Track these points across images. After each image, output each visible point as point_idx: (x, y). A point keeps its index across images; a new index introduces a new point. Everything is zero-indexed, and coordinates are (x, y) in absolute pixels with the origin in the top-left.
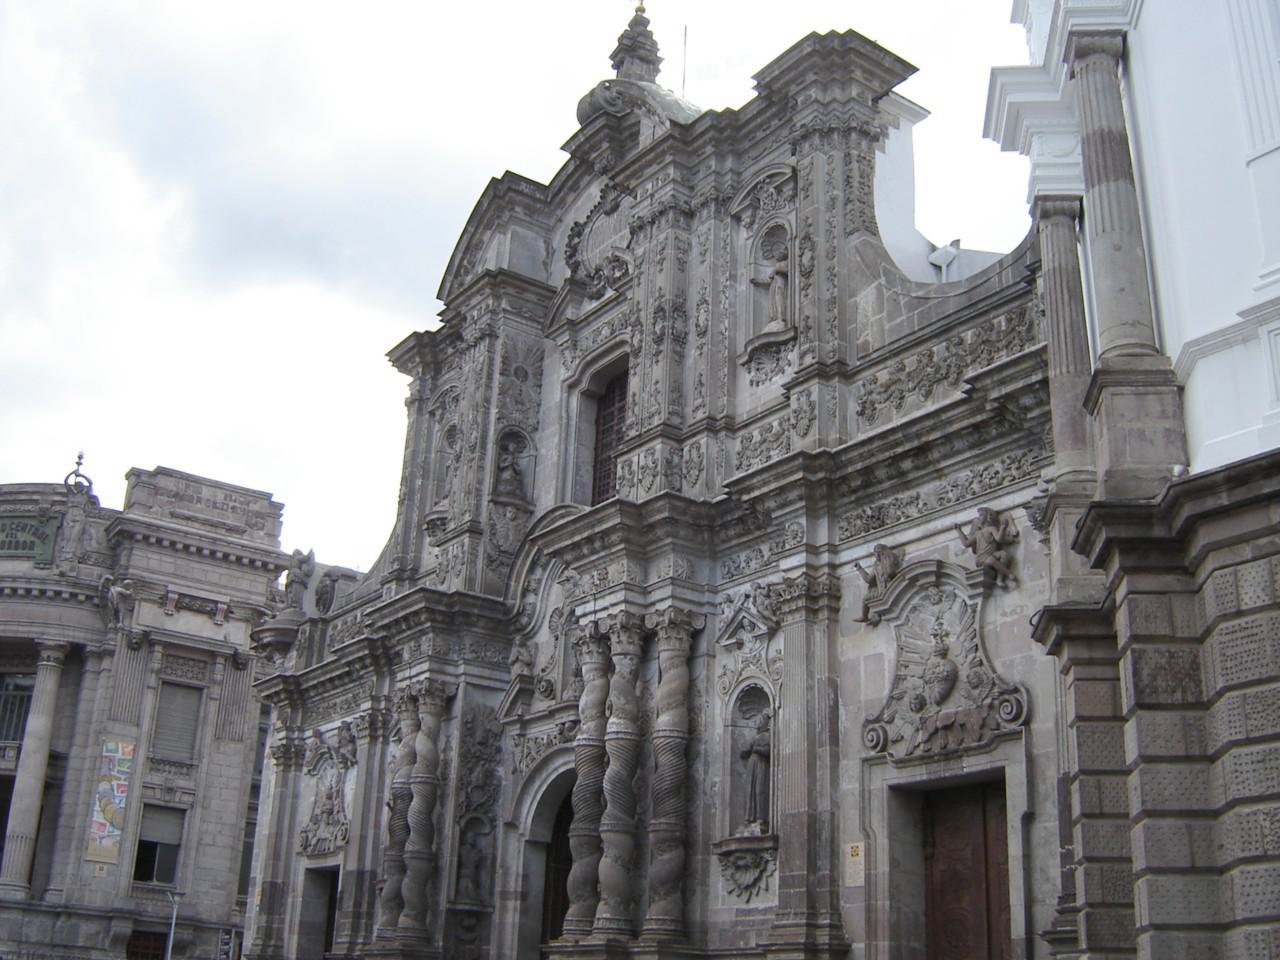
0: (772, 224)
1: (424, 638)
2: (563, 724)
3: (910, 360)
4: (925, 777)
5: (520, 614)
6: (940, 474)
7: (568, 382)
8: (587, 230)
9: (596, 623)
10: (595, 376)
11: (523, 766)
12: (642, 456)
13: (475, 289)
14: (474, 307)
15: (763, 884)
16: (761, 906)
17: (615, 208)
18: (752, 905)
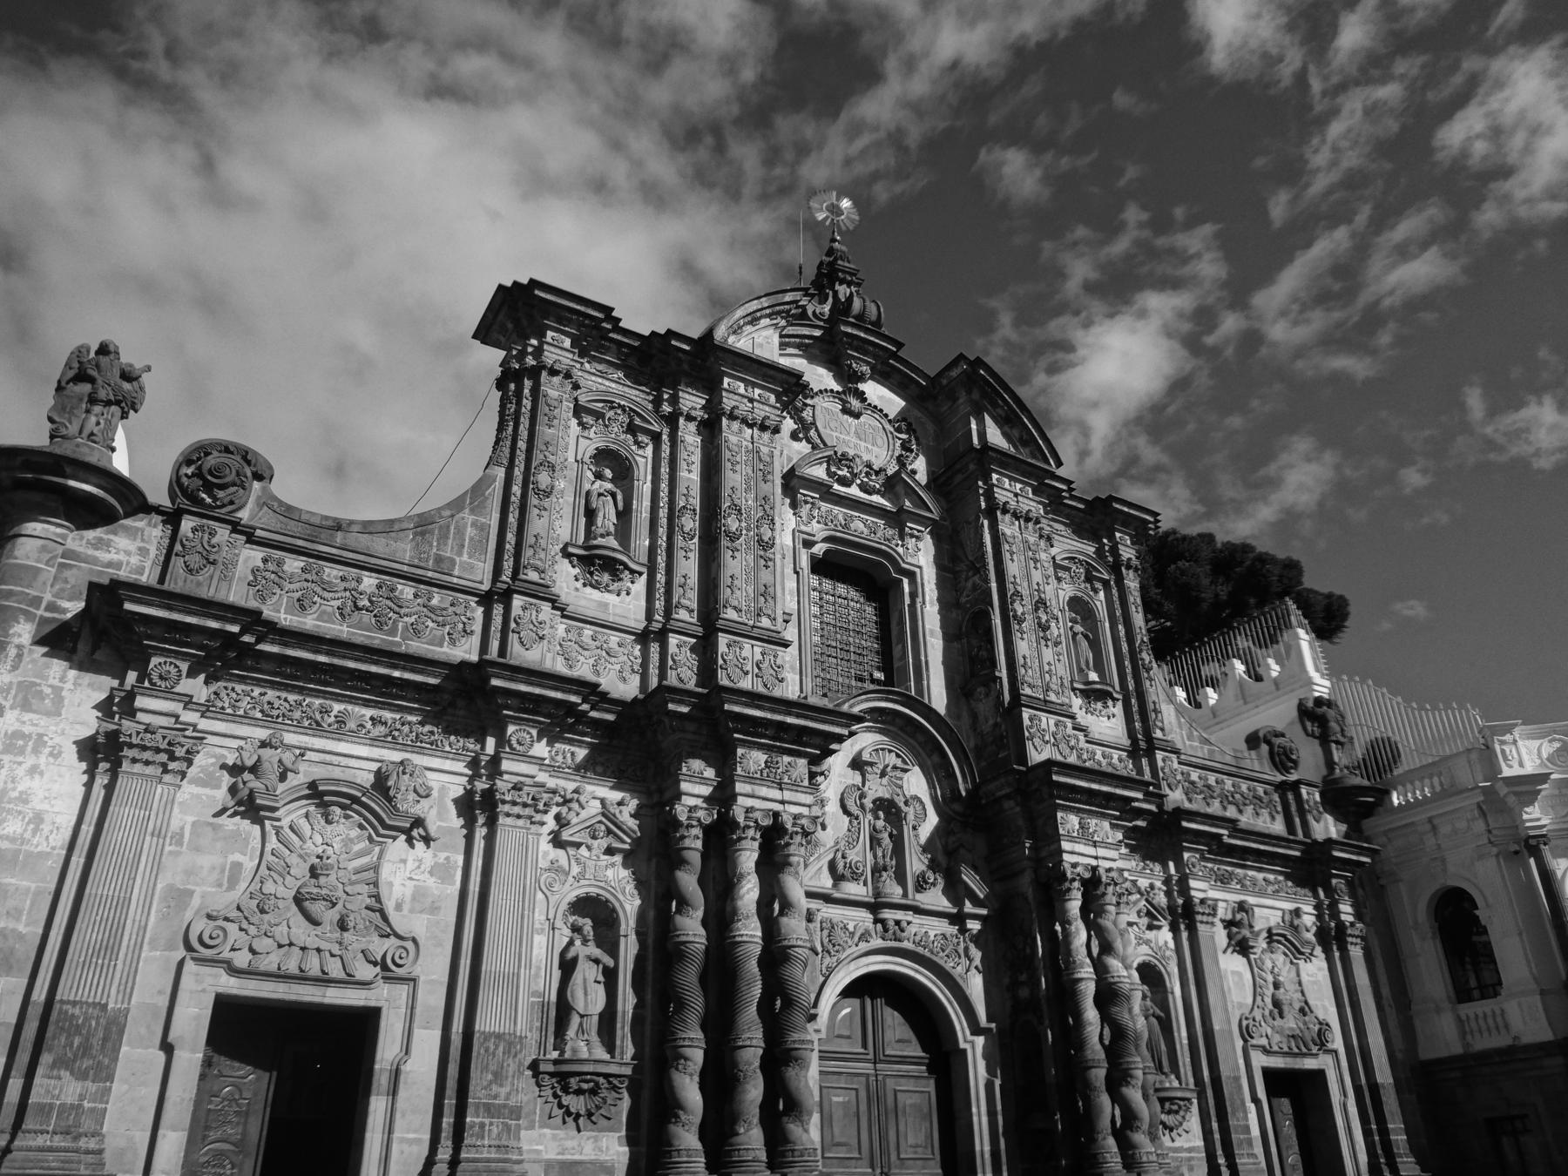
0: (1080, 594)
1: (787, 759)
2: (898, 923)
3: (1212, 779)
4: (1282, 1066)
5: (822, 774)
6: (1260, 870)
7: (806, 536)
8: (817, 400)
9: (1094, 869)
10: (827, 552)
11: (819, 949)
12: (1052, 722)
13: (772, 372)
14: (742, 380)
15: (1185, 1126)
16: (1186, 1145)
17: (857, 416)
18: (1177, 1144)
